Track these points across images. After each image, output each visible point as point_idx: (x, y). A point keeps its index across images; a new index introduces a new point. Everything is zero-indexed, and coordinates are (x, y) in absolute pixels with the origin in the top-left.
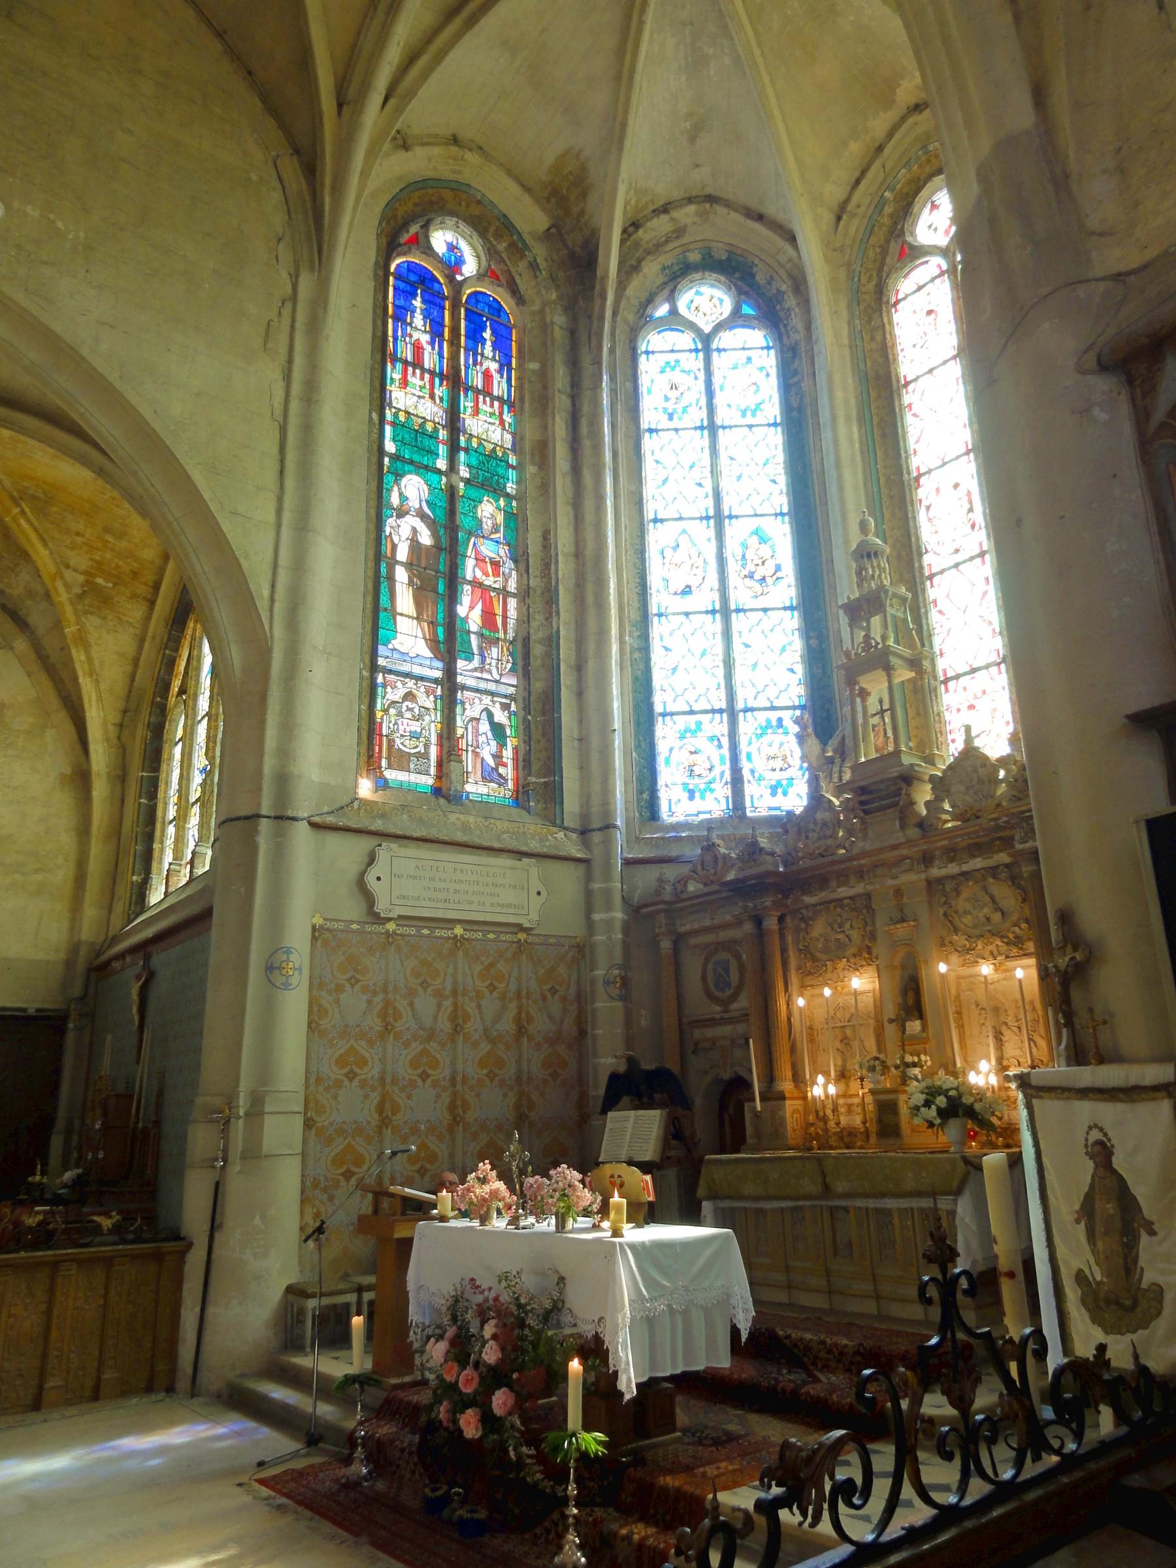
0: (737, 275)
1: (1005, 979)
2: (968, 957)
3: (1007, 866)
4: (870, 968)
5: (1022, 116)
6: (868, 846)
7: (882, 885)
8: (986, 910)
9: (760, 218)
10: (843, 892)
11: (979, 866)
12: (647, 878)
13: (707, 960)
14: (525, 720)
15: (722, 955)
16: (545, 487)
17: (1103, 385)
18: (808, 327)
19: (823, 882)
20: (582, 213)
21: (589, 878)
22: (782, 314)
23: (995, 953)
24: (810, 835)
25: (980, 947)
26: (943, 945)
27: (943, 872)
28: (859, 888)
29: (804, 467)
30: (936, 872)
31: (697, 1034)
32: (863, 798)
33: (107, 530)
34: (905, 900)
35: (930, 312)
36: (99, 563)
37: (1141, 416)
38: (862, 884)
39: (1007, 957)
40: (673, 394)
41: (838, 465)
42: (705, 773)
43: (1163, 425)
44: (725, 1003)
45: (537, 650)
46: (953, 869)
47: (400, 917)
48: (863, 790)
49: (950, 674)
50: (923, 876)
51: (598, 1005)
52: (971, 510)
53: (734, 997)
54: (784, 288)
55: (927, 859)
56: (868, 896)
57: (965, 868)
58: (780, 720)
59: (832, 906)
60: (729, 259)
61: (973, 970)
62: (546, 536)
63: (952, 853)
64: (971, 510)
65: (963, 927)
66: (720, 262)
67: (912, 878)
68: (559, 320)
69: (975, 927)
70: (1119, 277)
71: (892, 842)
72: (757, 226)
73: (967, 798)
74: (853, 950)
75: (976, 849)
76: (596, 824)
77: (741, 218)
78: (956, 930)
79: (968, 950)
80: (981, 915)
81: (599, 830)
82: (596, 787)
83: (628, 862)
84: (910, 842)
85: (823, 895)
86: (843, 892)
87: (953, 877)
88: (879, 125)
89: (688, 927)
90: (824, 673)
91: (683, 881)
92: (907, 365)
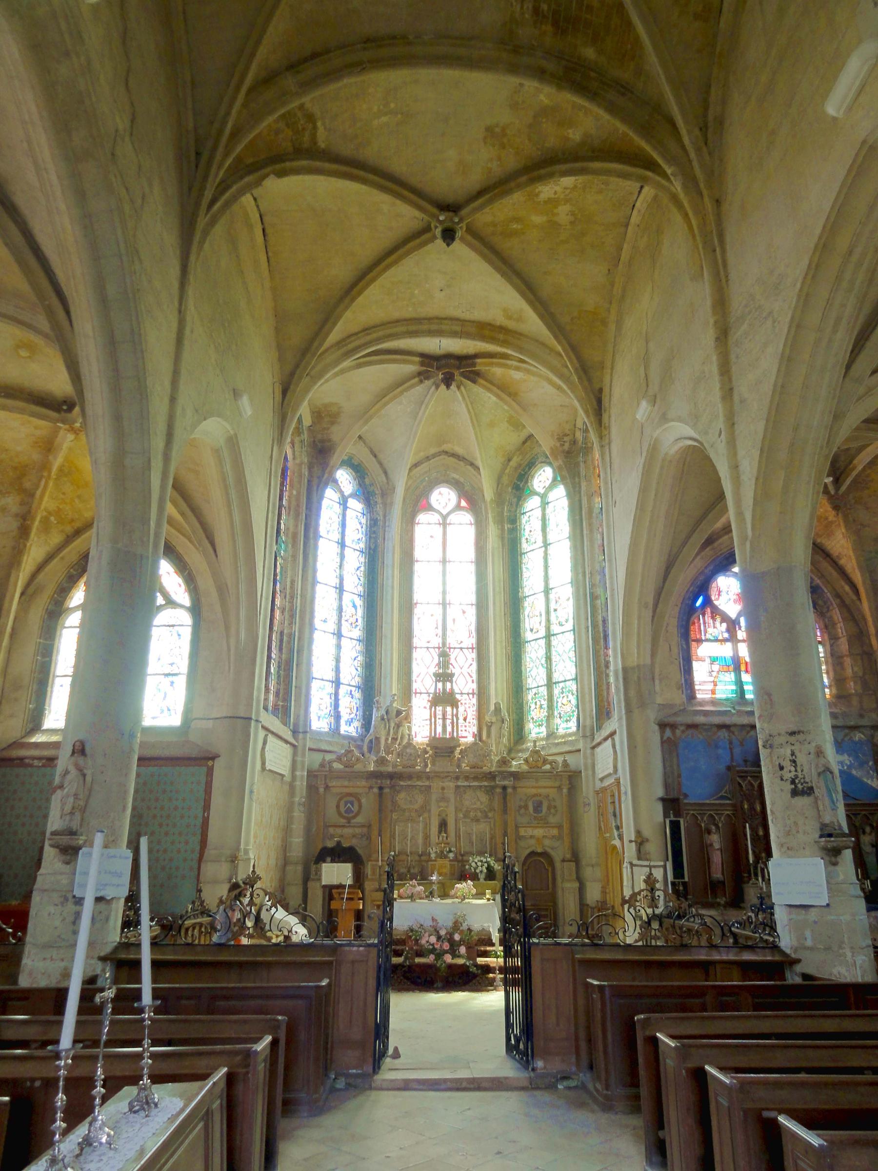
0: (358, 474)
3: (486, 786)
5: (648, 661)
6: (437, 769)
7: (436, 785)
9: (375, 456)
10: (420, 783)
12: (318, 758)
13: (340, 799)
14: (278, 672)
15: (351, 799)
16: (294, 557)
17: (657, 728)
18: (385, 516)
19: (410, 777)
20: (328, 429)
21: (295, 754)
22: (372, 502)
27: (463, 784)
28: (427, 783)
29: (373, 578)
30: (459, 783)
31: (331, 830)
32: (436, 751)
33: (79, 497)
34: (445, 791)
35: (431, 537)
36: (59, 510)
37: (662, 738)
40: (330, 521)
41: (393, 587)
42: (325, 709)
43: (665, 741)
44: (349, 820)
45: (285, 638)
46: (466, 784)
47: (270, 771)
48: (436, 748)
49: (418, 691)
51: (295, 814)
52: (437, 628)
53: (354, 817)
54: (377, 492)
55: (457, 778)
56: (430, 787)
57: (471, 784)
58: (351, 691)
60: (357, 466)
62: (293, 582)
63: (467, 778)
64: (437, 628)
66: (354, 464)
67: (452, 785)
68: (305, 472)
70: (659, 704)
72: (374, 459)
75: (476, 778)
76: (301, 730)
77: (369, 453)
81: (303, 733)
82: (302, 712)
83: (310, 749)
84: (456, 772)
85: (409, 783)
86: (420, 783)
87: (464, 786)
88: (433, 451)
89: (334, 784)
90: (370, 675)
91: (330, 762)
92: (418, 553)
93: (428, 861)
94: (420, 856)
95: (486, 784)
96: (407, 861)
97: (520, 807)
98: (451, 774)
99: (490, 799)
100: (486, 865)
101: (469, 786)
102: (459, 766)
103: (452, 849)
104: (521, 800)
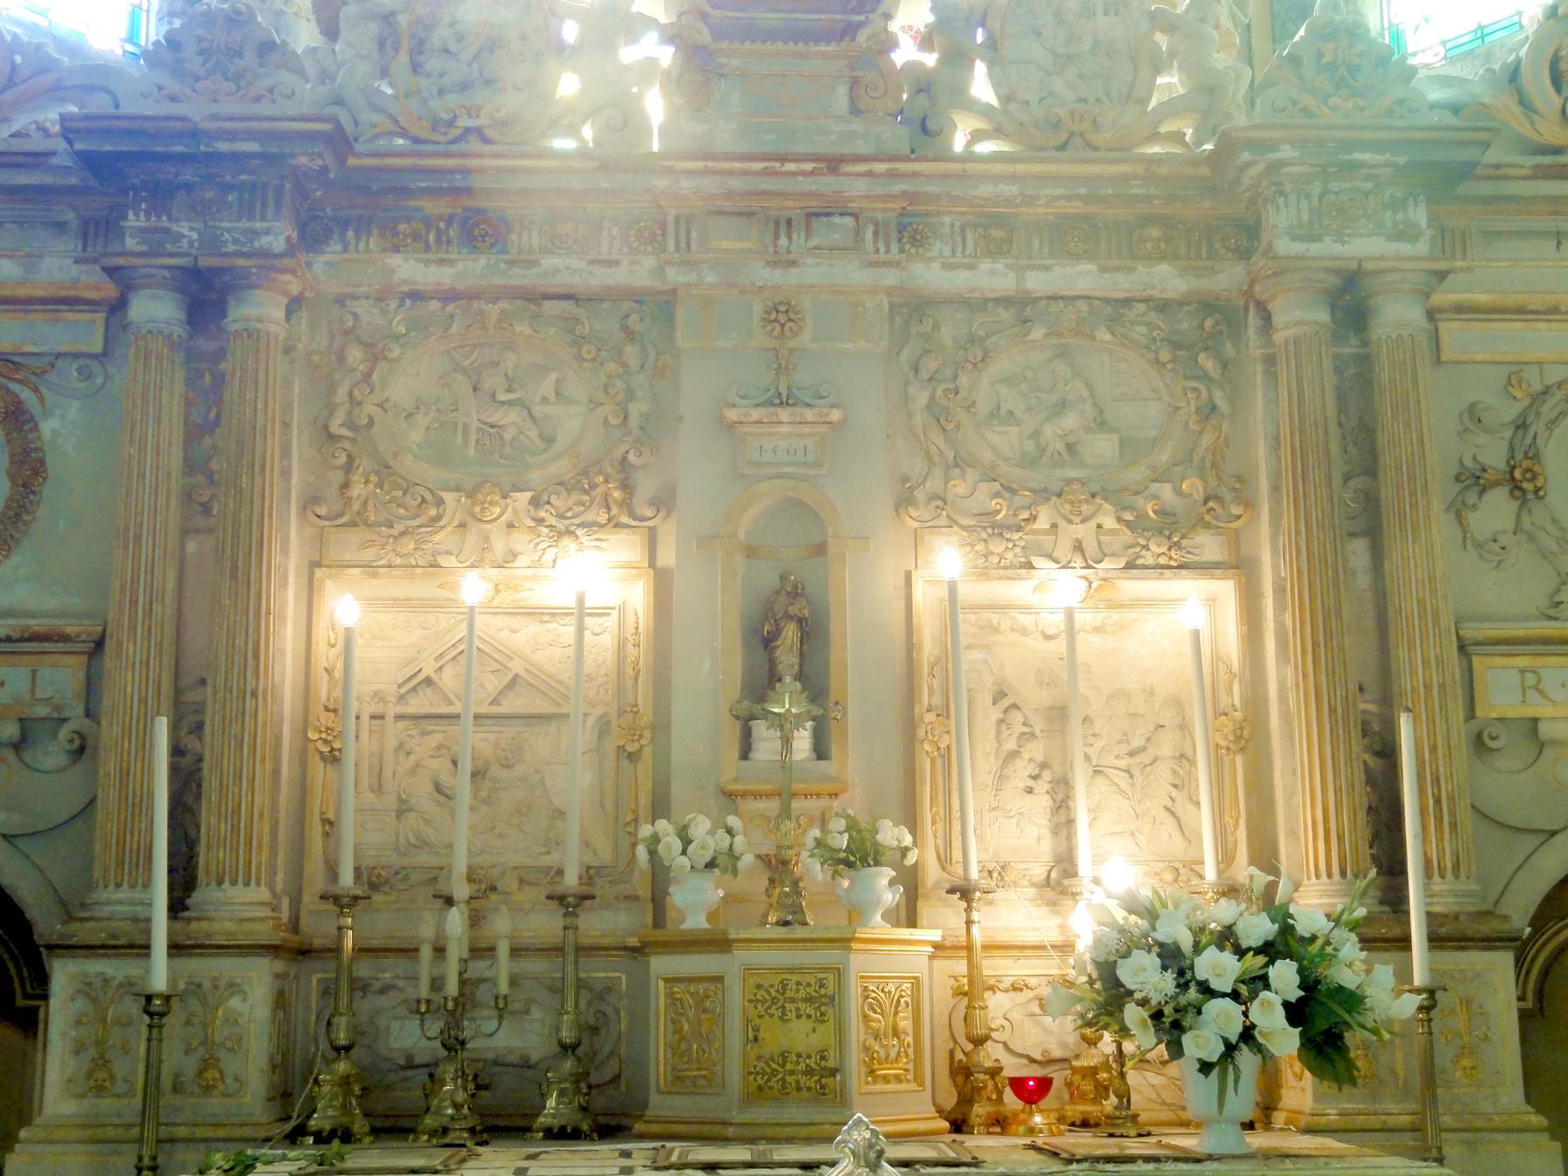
1: (1098, 630)
2: (998, 547)
3: (1164, 306)
4: (623, 536)
8: (1070, 421)
11: (1082, 286)
23: (1091, 547)
24: (432, 64)
25: (1042, 523)
26: (903, 502)
27: (958, 281)
38: (649, 262)
39: (1130, 566)
46: (995, 277)
50: (891, 278)
57: (1036, 283)
59: (493, 311)
61: (1019, 590)
65: (987, 456)
69: (1030, 462)
71: (825, 144)
73: (1058, 85)
74: (563, 468)
78: (959, 463)
79: (999, 530)
80: (1048, 430)
93: (638, 952)
94: (570, 904)
95: (1167, 279)
96: (440, 951)
97: (1474, 480)
98: (854, 187)
99: (1209, 411)
100: (1284, 975)
101: (1022, 306)
102: (927, 130)
103: (891, 834)
104: (1474, 415)
